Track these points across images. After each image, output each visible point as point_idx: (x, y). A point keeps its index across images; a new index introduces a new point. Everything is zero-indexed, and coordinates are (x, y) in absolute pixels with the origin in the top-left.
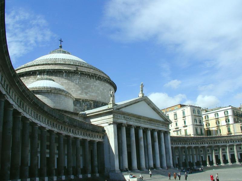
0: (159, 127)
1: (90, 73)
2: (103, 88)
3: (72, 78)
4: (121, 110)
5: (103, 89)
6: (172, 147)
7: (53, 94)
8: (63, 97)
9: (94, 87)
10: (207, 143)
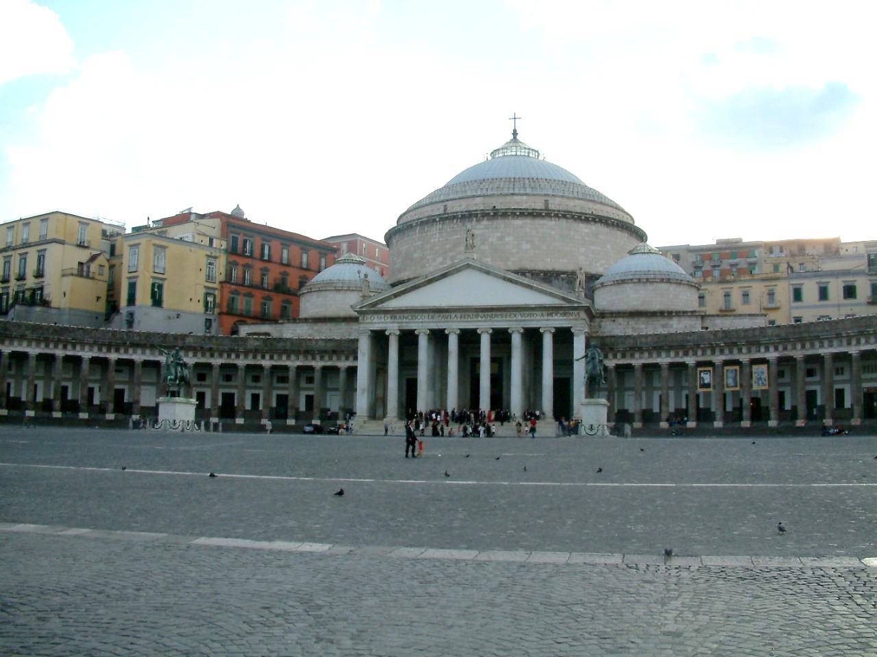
0: (525, 320)
1: (457, 212)
2: (499, 234)
3: (429, 234)
5: (501, 238)
7: (315, 293)
8: (330, 295)
10: (776, 349)
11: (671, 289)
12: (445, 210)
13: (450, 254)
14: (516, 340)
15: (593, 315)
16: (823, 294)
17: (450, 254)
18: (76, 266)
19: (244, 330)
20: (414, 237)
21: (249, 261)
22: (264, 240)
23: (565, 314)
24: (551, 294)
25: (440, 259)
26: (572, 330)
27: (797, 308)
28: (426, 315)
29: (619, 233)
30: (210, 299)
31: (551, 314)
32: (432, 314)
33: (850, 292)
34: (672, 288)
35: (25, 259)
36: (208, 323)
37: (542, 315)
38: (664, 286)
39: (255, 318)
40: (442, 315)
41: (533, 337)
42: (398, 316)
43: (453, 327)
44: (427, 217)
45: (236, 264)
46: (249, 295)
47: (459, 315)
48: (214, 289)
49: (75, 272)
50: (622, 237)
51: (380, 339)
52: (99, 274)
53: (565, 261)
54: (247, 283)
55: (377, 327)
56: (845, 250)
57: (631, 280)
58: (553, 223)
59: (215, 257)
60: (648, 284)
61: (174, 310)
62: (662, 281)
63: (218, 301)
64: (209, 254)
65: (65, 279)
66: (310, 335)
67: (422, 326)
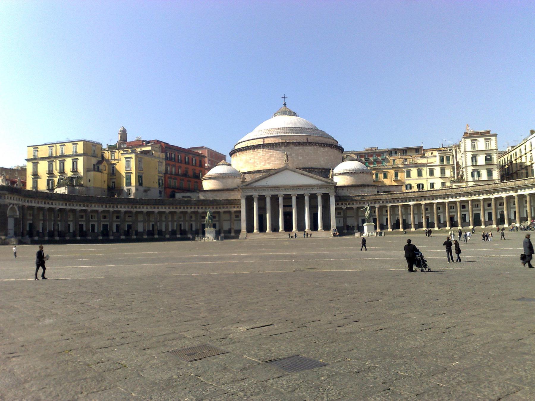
0: (310, 191)
3: (257, 152)
4: (251, 185)
6: (336, 209)
9: (277, 155)
11: (364, 176)
12: (264, 141)
13: (268, 161)
14: (307, 198)
15: (337, 188)
16: (420, 174)
17: (268, 161)
18: (92, 167)
19: (179, 196)
20: (249, 153)
21: (173, 163)
22: (178, 153)
23: (326, 188)
24: (321, 180)
25: (263, 163)
26: (329, 194)
27: (408, 180)
28: (269, 189)
29: (335, 150)
30: (161, 182)
31: (321, 188)
32: (272, 189)
33: (431, 173)
34: (365, 175)
35: (64, 163)
36: (160, 192)
37: (317, 188)
38: (361, 175)
39: (178, 189)
40: (276, 189)
41: (313, 197)
42: (257, 189)
43: (281, 194)
44: (257, 145)
45: (169, 165)
46: (176, 179)
47: (283, 189)
48: (162, 177)
49: (92, 169)
50: (336, 152)
51: (249, 200)
52: (104, 170)
53: (316, 164)
54: (173, 173)
55: (249, 194)
56: (427, 154)
57: (348, 173)
58: (311, 148)
59: (161, 162)
60: (355, 174)
61: (148, 187)
62: (361, 172)
63: (163, 182)
64: (159, 161)
65: (89, 173)
66: (212, 197)
67: (268, 194)
